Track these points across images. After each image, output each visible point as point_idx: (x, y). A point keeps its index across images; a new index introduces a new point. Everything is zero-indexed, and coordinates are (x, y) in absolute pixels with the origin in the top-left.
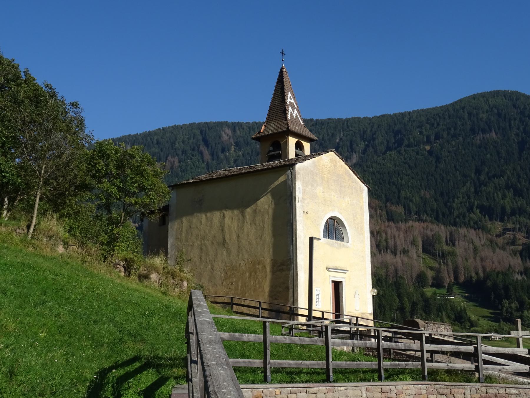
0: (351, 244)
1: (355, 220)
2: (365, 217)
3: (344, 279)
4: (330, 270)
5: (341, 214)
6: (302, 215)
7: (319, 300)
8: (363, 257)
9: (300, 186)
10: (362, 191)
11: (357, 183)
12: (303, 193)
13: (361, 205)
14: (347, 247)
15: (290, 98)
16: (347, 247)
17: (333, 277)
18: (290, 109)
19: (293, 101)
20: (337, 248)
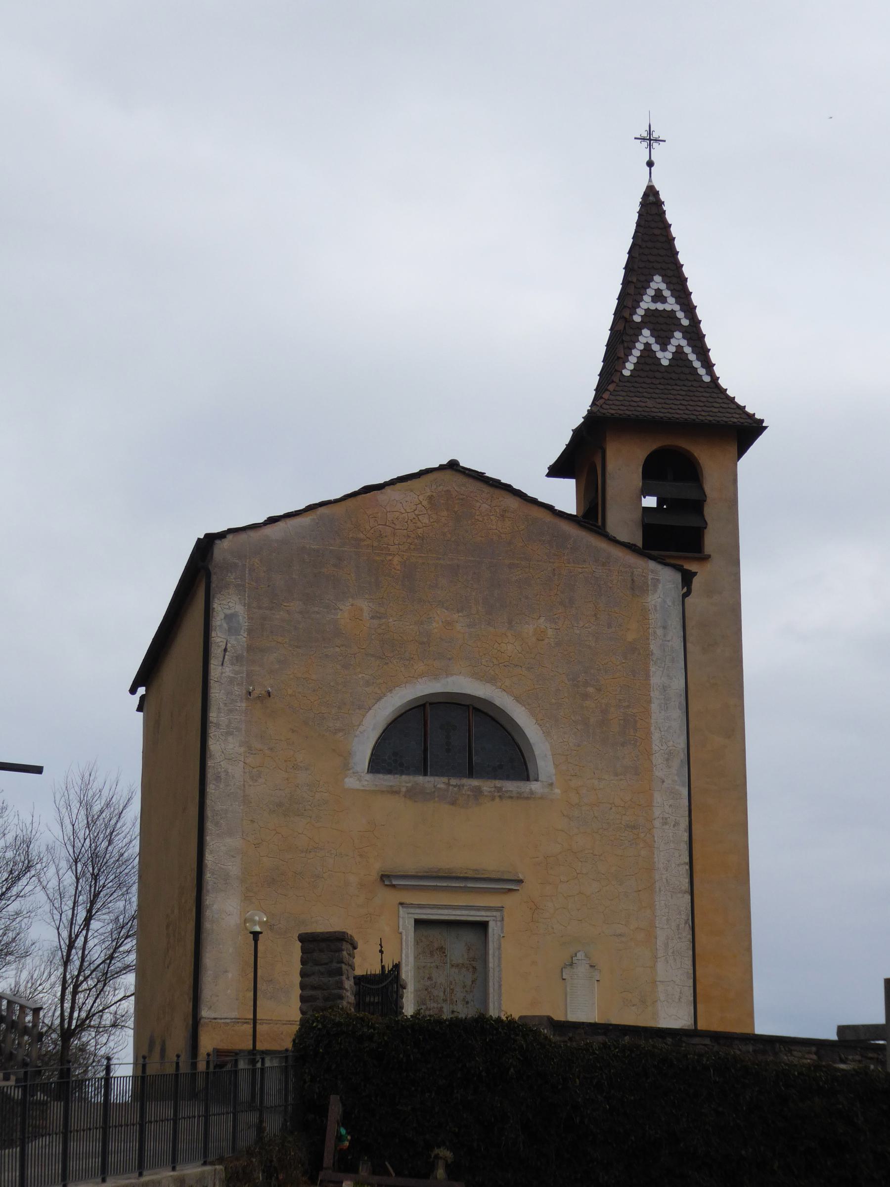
1: (586, 696)
2: (656, 679)
3: (497, 914)
5: (492, 680)
8: (634, 827)
9: (239, 609)
10: (638, 588)
12: (250, 631)
13: (631, 637)
15: (658, 297)
16: (530, 797)
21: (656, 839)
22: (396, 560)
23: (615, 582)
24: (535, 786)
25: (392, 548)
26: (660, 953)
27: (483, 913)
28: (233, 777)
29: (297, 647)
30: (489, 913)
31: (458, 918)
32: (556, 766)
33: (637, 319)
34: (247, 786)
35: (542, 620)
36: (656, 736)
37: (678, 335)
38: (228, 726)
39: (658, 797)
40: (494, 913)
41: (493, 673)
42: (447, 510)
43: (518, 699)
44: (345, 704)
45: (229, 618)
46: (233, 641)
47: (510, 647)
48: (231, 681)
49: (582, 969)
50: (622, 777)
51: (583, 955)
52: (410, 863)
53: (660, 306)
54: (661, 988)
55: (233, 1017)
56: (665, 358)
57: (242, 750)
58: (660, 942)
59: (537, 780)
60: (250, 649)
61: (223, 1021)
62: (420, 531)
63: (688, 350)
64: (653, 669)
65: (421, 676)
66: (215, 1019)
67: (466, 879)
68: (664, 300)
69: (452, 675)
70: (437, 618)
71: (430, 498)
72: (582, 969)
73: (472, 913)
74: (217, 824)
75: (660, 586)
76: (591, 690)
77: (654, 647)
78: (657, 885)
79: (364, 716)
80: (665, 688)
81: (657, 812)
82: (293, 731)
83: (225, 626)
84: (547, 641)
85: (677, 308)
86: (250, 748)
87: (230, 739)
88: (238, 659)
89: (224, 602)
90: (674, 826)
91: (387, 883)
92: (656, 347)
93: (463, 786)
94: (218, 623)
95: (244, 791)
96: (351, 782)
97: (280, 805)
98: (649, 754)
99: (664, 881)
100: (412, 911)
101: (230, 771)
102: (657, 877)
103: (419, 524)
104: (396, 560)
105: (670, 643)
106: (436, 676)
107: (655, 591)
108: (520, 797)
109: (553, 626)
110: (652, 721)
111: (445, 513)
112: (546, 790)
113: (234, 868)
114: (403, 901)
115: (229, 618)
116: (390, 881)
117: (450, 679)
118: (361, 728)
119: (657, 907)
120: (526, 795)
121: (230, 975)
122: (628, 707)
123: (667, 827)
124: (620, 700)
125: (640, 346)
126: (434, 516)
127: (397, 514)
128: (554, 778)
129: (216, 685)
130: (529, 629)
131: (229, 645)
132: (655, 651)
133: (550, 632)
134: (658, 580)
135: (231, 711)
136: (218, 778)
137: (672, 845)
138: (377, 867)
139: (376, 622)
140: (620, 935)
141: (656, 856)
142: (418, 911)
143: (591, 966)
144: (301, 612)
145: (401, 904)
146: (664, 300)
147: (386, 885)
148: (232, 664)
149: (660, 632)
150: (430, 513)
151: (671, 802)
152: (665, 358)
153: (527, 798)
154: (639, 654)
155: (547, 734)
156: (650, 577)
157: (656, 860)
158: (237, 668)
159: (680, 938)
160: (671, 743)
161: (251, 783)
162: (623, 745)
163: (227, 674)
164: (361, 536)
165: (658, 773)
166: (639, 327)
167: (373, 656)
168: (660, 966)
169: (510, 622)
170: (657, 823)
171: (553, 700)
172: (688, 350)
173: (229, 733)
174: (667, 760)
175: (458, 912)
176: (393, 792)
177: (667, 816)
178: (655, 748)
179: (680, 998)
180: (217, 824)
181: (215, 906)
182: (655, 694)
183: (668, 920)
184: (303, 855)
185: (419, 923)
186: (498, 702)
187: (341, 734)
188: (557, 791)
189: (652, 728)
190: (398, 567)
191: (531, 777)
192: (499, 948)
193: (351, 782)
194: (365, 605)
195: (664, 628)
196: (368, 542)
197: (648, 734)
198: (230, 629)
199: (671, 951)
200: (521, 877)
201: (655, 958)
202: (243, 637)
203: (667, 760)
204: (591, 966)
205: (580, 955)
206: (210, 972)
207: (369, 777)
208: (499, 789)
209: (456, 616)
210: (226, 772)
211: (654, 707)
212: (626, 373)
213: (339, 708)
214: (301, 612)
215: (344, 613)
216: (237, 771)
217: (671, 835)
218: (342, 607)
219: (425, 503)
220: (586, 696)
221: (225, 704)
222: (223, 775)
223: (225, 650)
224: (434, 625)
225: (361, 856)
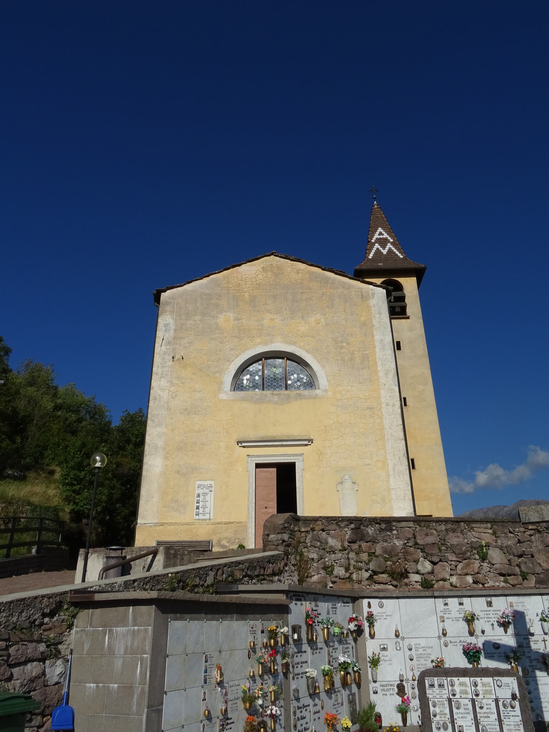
0: (326, 391)
1: (342, 348)
2: (377, 337)
4: (244, 444)
5: (294, 343)
6: (170, 363)
7: (208, 504)
8: (371, 408)
10: (364, 297)
11: (349, 287)
12: (175, 330)
13: (363, 319)
14: (315, 397)
15: (381, 234)
16: (315, 397)
17: (258, 456)
18: (377, 246)
19: (386, 235)
20: (276, 403)
21: (383, 413)
22: (247, 295)
23: (353, 296)
24: (317, 392)
25: (244, 290)
26: (391, 473)
27: (292, 458)
28: (163, 398)
29: (198, 335)
30: (295, 458)
31: (279, 461)
32: (328, 381)
33: (373, 241)
34: (169, 402)
35: (318, 315)
36: (379, 363)
37: (389, 244)
38: (162, 374)
39: (383, 393)
40: (299, 457)
41: (294, 340)
42: (271, 272)
43: (307, 351)
44: (220, 360)
45: (166, 325)
46: (167, 335)
47: (303, 328)
48: (165, 353)
49: (348, 484)
50: (363, 384)
51: (348, 476)
52: (252, 435)
53: (381, 237)
54: (393, 492)
55: (155, 522)
56: (385, 252)
57: (168, 384)
58: (391, 466)
59: (319, 389)
60: (174, 338)
61: (149, 525)
62: (258, 282)
63: (393, 248)
64: (375, 332)
65: (259, 344)
66: (145, 524)
67: (281, 441)
68: (383, 235)
69: (274, 343)
70: (266, 318)
71: (263, 268)
72: (348, 484)
73: (287, 458)
74: (153, 421)
75: (376, 296)
76: (344, 344)
77: (375, 322)
78: (386, 437)
79: (230, 364)
80: (382, 341)
81: (383, 400)
82: (194, 374)
83: (164, 328)
84: (321, 324)
85: (388, 236)
86: (172, 383)
87: (163, 380)
88: (169, 343)
89: (164, 319)
90: (393, 406)
91: (240, 445)
92: (381, 249)
93: (280, 394)
94: (161, 328)
95: (168, 404)
96: (223, 396)
97: (186, 409)
98: (376, 372)
99: (390, 434)
100: (254, 459)
101: (161, 395)
102: (386, 433)
103: (258, 279)
104: (247, 295)
105: (383, 320)
106: (266, 344)
107: (373, 298)
108: (310, 397)
109: (324, 317)
110: (377, 356)
111: (270, 273)
112: (324, 394)
113: (160, 443)
114: (248, 454)
115: (166, 325)
116: (241, 444)
117: (273, 345)
118: (228, 370)
119: (387, 448)
120: (313, 396)
121: (154, 499)
122: (364, 351)
123: (389, 407)
124: (359, 348)
125: (375, 249)
126: (265, 275)
127: (247, 276)
128: (328, 387)
129: (158, 355)
130: (312, 320)
131: (165, 337)
132: (376, 324)
133: (322, 320)
134: (374, 293)
135: (163, 367)
136: (155, 399)
137: (393, 416)
138: (236, 437)
139: (236, 322)
140: (368, 465)
141: (384, 422)
142: (257, 459)
143: (353, 483)
144: (200, 320)
145: (248, 456)
146: (383, 235)
147: (240, 447)
148: (166, 345)
149: (377, 316)
150: (263, 273)
151: (390, 394)
152: (385, 252)
153: (314, 398)
154: (368, 326)
155: (323, 367)
156: (370, 292)
157: (384, 424)
158: (168, 347)
159: (401, 464)
160: (387, 366)
161: (171, 400)
162: (363, 369)
163: (163, 350)
164: (230, 286)
165: (382, 381)
166: (374, 244)
167: (235, 337)
168: (392, 480)
169: (302, 317)
170: (384, 405)
171: (326, 351)
172: (393, 248)
173: (161, 377)
174: (386, 374)
175: (279, 458)
176: (244, 399)
177: (388, 401)
178: (379, 369)
179: (404, 497)
180: (153, 421)
181: (149, 463)
182: (377, 344)
183: (394, 455)
184: (197, 434)
185: (258, 466)
186: (297, 353)
187: (218, 374)
188: (330, 393)
189: (377, 360)
190: (248, 297)
191: (317, 387)
192: (302, 476)
193: (223, 396)
194: (231, 315)
195: (380, 313)
196: (234, 288)
197: (376, 363)
198: (166, 330)
199: (397, 471)
200: (312, 438)
201: (388, 476)
202: (172, 333)
203: (386, 374)
204: (353, 483)
205: (346, 477)
206: (143, 498)
207: (232, 393)
208: (300, 394)
209: (276, 316)
210: (160, 395)
211: (377, 350)
212: (370, 257)
213: (217, 361)
214: (200, 320)
215: (221, 320)
216: (165, 395)
217: (391, 411)
218: (220, 316)
219: (261, 270)
220: (342, 348)
221: (161, 364)
222: (158, 397)
223: (163, 339)
224: (265, 321)
225: (227, 432)
